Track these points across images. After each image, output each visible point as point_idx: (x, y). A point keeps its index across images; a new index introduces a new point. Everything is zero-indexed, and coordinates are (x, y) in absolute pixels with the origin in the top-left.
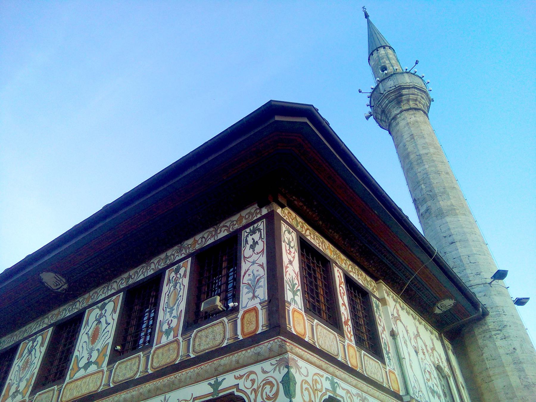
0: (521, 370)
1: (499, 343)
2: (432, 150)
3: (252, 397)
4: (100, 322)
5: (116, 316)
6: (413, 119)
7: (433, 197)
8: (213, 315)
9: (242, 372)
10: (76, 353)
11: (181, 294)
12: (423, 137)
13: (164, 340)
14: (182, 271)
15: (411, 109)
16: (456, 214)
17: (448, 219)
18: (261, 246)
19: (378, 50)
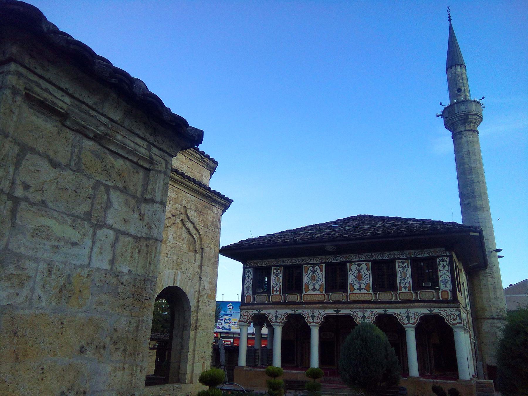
0: (496, 292)
1: (489, 279)
2: (478, 165)
3: (447, 317)
4: (359, 272)
5: (370, 271)
6: (471, 138)
7: (474, 197)
8: (428, 288)
9: (442, 309)
10: (349, 282)
11: (408, 274)
12: (475, 154)
13: (403, 290)
14: (406, 264)
15: (471, 130)
16: (483, 211)
17: (479, 213)
18: (447, 268)
19: (456, 67)
